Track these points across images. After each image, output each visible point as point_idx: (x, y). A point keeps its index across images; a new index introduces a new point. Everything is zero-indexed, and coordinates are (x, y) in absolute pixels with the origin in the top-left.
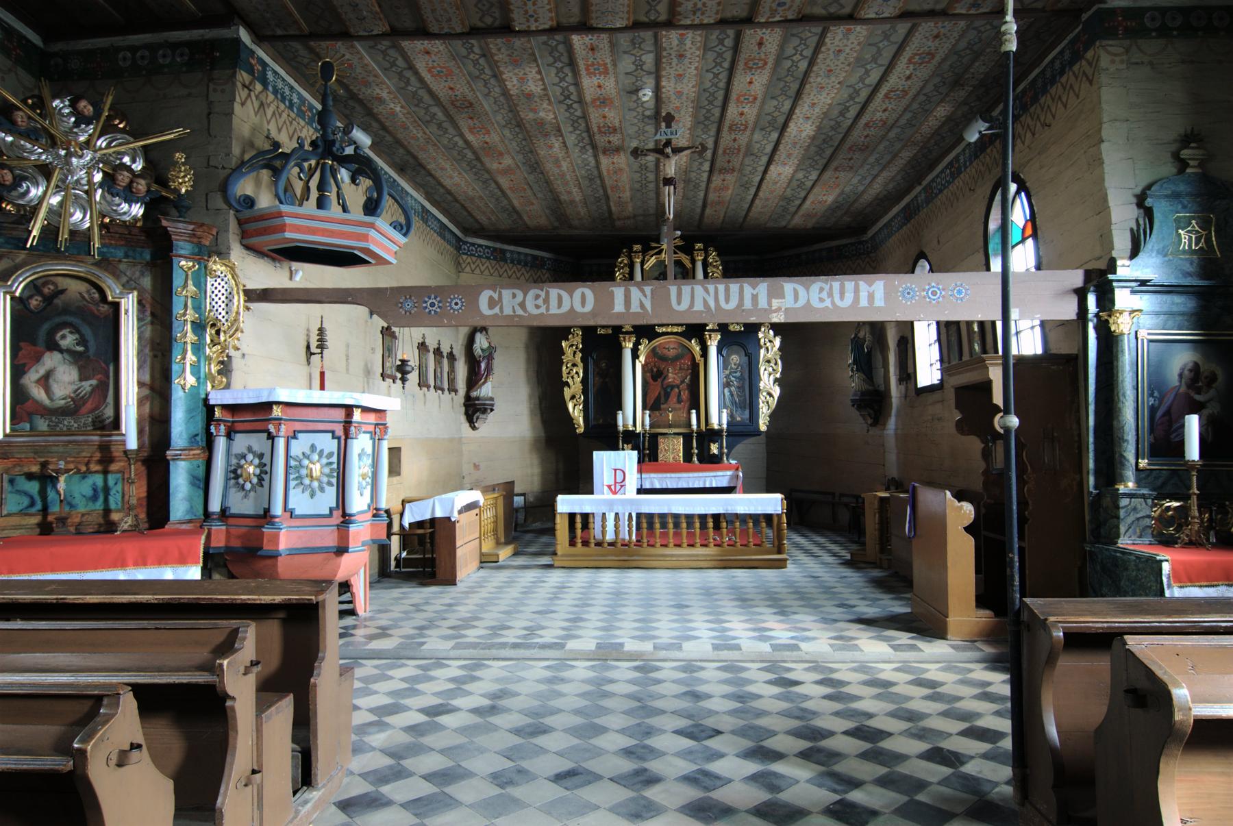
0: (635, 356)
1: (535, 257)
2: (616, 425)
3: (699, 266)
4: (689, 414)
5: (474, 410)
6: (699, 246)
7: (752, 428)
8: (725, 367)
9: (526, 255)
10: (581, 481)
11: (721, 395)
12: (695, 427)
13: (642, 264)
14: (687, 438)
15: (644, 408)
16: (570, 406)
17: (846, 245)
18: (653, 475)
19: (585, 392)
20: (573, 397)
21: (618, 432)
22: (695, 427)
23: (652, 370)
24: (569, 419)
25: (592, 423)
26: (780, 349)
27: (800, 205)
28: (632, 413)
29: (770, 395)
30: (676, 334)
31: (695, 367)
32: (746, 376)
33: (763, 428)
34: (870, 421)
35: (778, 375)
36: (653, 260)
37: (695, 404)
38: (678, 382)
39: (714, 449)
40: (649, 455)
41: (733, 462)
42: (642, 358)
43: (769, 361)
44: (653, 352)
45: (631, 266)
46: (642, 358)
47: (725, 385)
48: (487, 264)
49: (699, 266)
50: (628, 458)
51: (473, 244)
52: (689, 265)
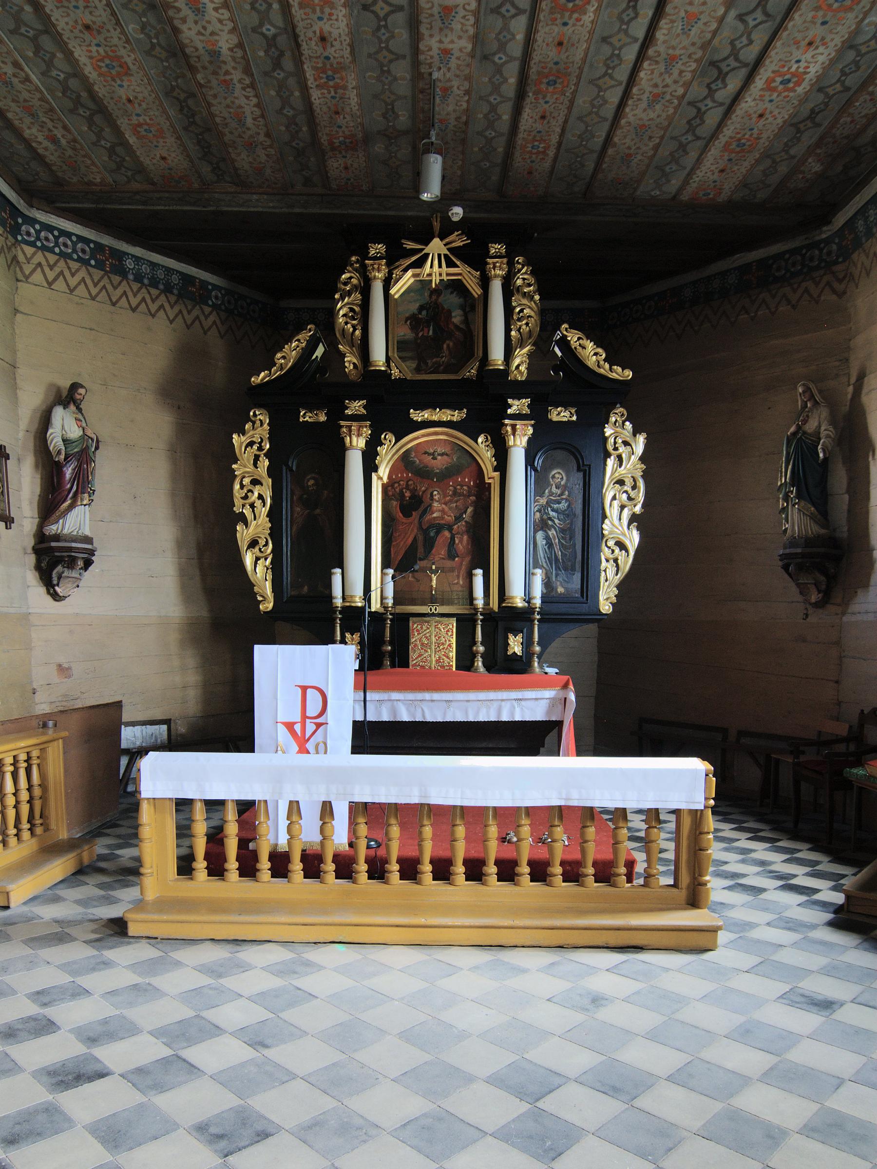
0: (370, 466)
2: (330, 597)
3: (496, 288)
4: (470, 577)
5: (56, 560)
6: (495, 248)
7: (584, 608)
8: (539, 492)
11: (531, 545)
12: (480, 603)
13: (388, 283)
14: (465, 624)
15: (385, 565)
16: (248, 560)
18: (395, 695)
19: (275, 534)
21: (334, 609)
22: (480, 603)
23: (402, 495)
25: (289, 592)
26: (642, 459)
28: (363, 575)
29: (621, 546)
31: (482, 490)
32: (578, 507)
34: (814, 597)
35: (638, 509)
37: (480, 557)
38: (449, 518)
39: (515, 645)
40: (392, 654)
41: (552, 671)
42: (384, 471)
43: (621, 482)
44: (405, 461)
45: (366, 291)
46: (384, 471)
48: (83, 273)
49: (496, 288)
51: (50, 228)
52: (476, 291)
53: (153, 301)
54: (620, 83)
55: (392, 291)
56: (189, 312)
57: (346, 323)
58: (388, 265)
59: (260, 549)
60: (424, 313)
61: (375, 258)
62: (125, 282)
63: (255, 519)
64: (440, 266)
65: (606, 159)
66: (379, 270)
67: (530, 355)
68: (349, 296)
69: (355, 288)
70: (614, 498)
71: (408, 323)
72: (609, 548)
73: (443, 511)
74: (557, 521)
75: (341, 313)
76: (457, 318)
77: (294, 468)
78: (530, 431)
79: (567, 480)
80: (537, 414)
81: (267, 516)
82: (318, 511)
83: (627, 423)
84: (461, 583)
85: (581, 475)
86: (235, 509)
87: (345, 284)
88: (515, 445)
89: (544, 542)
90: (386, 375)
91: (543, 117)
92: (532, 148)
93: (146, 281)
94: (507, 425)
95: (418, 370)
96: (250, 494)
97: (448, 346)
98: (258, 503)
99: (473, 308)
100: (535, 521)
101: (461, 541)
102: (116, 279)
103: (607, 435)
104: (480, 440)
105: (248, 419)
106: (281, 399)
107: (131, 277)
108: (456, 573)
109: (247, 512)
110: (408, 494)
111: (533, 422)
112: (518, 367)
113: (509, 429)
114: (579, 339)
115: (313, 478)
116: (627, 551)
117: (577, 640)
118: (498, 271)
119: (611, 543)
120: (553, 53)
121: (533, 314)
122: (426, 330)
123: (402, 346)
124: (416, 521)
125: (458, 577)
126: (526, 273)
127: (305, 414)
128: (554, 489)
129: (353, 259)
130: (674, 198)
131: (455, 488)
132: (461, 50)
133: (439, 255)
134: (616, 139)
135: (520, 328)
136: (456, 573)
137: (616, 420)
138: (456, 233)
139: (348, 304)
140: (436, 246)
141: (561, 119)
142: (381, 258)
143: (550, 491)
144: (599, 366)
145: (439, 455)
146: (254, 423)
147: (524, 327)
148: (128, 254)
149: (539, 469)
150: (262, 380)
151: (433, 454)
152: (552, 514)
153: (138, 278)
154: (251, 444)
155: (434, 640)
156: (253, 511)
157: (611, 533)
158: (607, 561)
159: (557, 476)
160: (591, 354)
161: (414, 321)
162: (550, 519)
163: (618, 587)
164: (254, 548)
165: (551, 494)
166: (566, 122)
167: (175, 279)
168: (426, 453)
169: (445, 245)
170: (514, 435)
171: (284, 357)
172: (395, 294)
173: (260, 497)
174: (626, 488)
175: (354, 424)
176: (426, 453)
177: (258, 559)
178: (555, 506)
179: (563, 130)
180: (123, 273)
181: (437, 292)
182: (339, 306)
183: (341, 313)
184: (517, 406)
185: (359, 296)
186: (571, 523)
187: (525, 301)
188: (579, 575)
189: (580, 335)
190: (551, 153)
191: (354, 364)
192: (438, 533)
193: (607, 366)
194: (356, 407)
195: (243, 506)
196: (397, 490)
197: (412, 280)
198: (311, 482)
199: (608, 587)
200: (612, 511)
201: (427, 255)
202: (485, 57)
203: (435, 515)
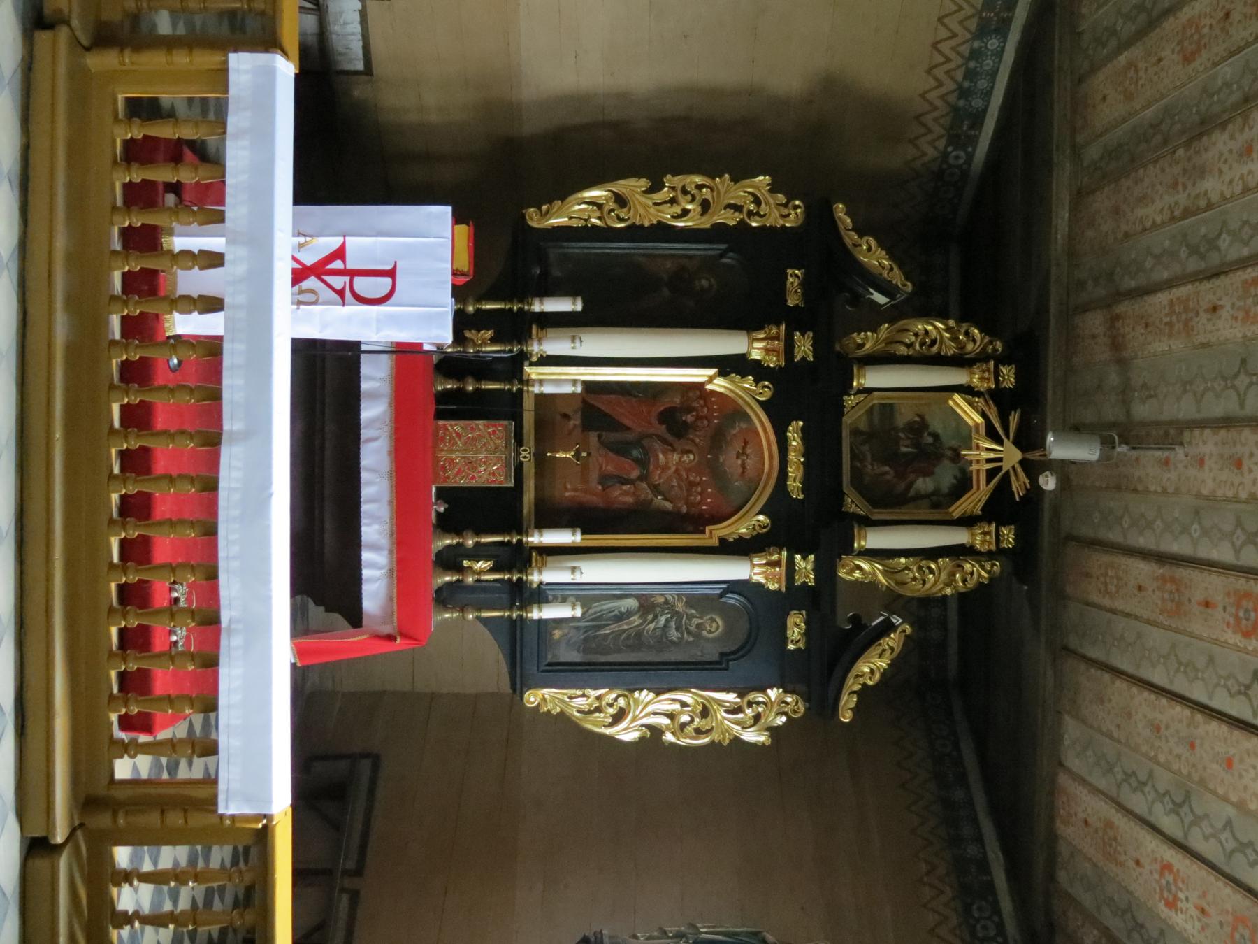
0: (727, 365)
1: (978, 119)
3: (958, 537)
6: (1009, 536)
7: (531, 668)
8: (692, 601)
9: (988, 94)
10: (345, 155)
13: (966, 390)
15: (589, 387)
17: (997, 911)
19: (635, 233)
20: (621, 201)
23: (689, 410)
24: (564, 190)
26: (737, 740)
27: (1155, 829)
29: (619, 717)
31: (696, 522)
33: (532, 698)
36: (973, 417)
38: (656, 477)
42: (720, 385)
43: (705, 713)
45: (959, 361)
46: (720, 385)
47: (647, 600)
49: (958, 537)
50: (423, 316)
52: (957, 510)
53: (948, 72)
54: (1171, 682)
55: (957, 397)
56: (936, 120)
57: (916, 335)
58: (989, 391)
59: (612, 210)
60: (930, 440)
61: (997, 373)
62: (969, 36)
63: (656, 204)
64: (989, 461)
65: (1099, 672)
66: (982, 379)
67: (873, 586)
68: (952, 339)
69: (962, 347)
70: (684, 704)
71: (917, 419)
72: (616, 700)
73: (666, 468)
74: (652, 626)
75: (929, 328)
76: (923, 485)
77: (725, 260)
78: (773, 586)
79: (708, 640)
80: (794, 596)
81: (659, 222)
82: (666, 292)
83: (784, 719)
84: (567, 494)
85: (715, 658)
86: (669, 176)
87: (967, 334)
88: (753, 566)
89: (623, 610)
90: (846, 387)
91: (1140, 588)
92: (1112, 578)
93: (972, 64)
94: (780, 554)
95: (855, 432)
96: (689, 197)
97: (886, 473)
98: (677, 210)
99: (936, 506)
100: (652, 596)
101: (626, 493)
102: (973, 24)
103: (769, 691)
104: (761, 518)
105: (790, 198)
106: (818, 246)
107: (976, 44)
108: (580, 486)
109: (664, 194)
110: (689, 418)
111: (783, 589)
112: (859, 568)
113: (775, 557)
114: (892, 649)
115: (711, 286)
116: (611, 725)
117: (486, 664)
118: (978, 538)
119: (622, 702)
120: (1198, 596)
121: (928, 586)
122: (908, 442)
123: (887, 410)
124: (652, 431)
125: (576, 490)
126: (980, 576)
127: (797, 276)
128: (695, 621)
129: (999, 345)
130: (1061, 764)
131: (699, 484)
132: (1203, 481)
133: (1000, 460)
134: (1118, 683)
135: (909, 569)
136: (580, 486)
137: (787, 704)
138: (1027, 481)
139: (942, 337)
140: (1011, 455)
141: (1137, 611)
142: (997, 381)
143: (693, 616)
144: (857, 676)
145: (743, 461)
146: (785, 206)
147: (911, 575)
148: (1005, 42)
149: (723, 600)
150: (840, 218)
151: (744, 453)
152: (662, 620)
153: (975, 55)
154: (757, 202)
155: (481, 456)
156: (666, 202)
157: (637, 702)
158: (599, 698)
159: (714, 625)
160: (872, 666)
161: (918, 428)
162: (656, 617)
163: (562, 713)
164: (615, 201)
165: (690, 617)
166: (1136, 618)
167: (977, 103)
168: (746, 443)
169: (1013, 467)
170: (768, 564)
171: (869, 249)
172: (954, 401)
173: (685, 212)
174: (697, 720)
175: (782, 344)
176: (746, 443)
177: (600, 207)
178: (673, 624)
179: (1128, 615)
180: (983, 31)
181: (956, 457)
182: (938, 324)
183: (929, 328)
184: (805, 566)
185: (950, 353)
186: (650, 647)
187: (943, 576)
188: (578, 660)
189: (897, 650)
190: (1106, 602)
191: (863, 345)
192: (637, 461)
193: (857, 687)
194: (804, 347)
195: (673, 189)
196: (695, 404)
197: (970, 423)
198: (704, 283)
199: (562, 701)
200: (666, 703)
201: (1000, 442)
202: (1197, 513)
203: (661, 456)
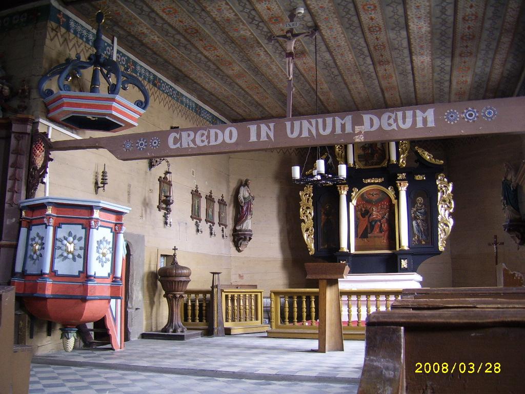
23: (361, 210)
26: (452, 192)
29: (447, 225)
30: (378, 184)
33: (441, 248)
43: (444, 201)
47: (410, 219)
74: (420, 217)
79: (424, 201)
104: (389, 189)
110: (363, 209)
116: (448, 227)
178: (419, 211)
199: (442, 241)
